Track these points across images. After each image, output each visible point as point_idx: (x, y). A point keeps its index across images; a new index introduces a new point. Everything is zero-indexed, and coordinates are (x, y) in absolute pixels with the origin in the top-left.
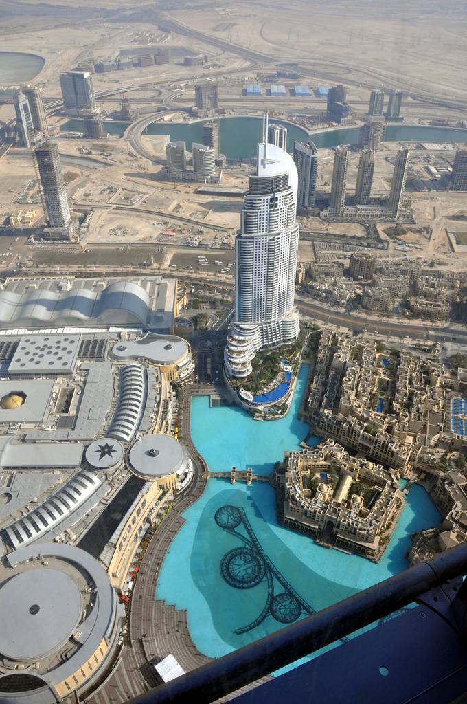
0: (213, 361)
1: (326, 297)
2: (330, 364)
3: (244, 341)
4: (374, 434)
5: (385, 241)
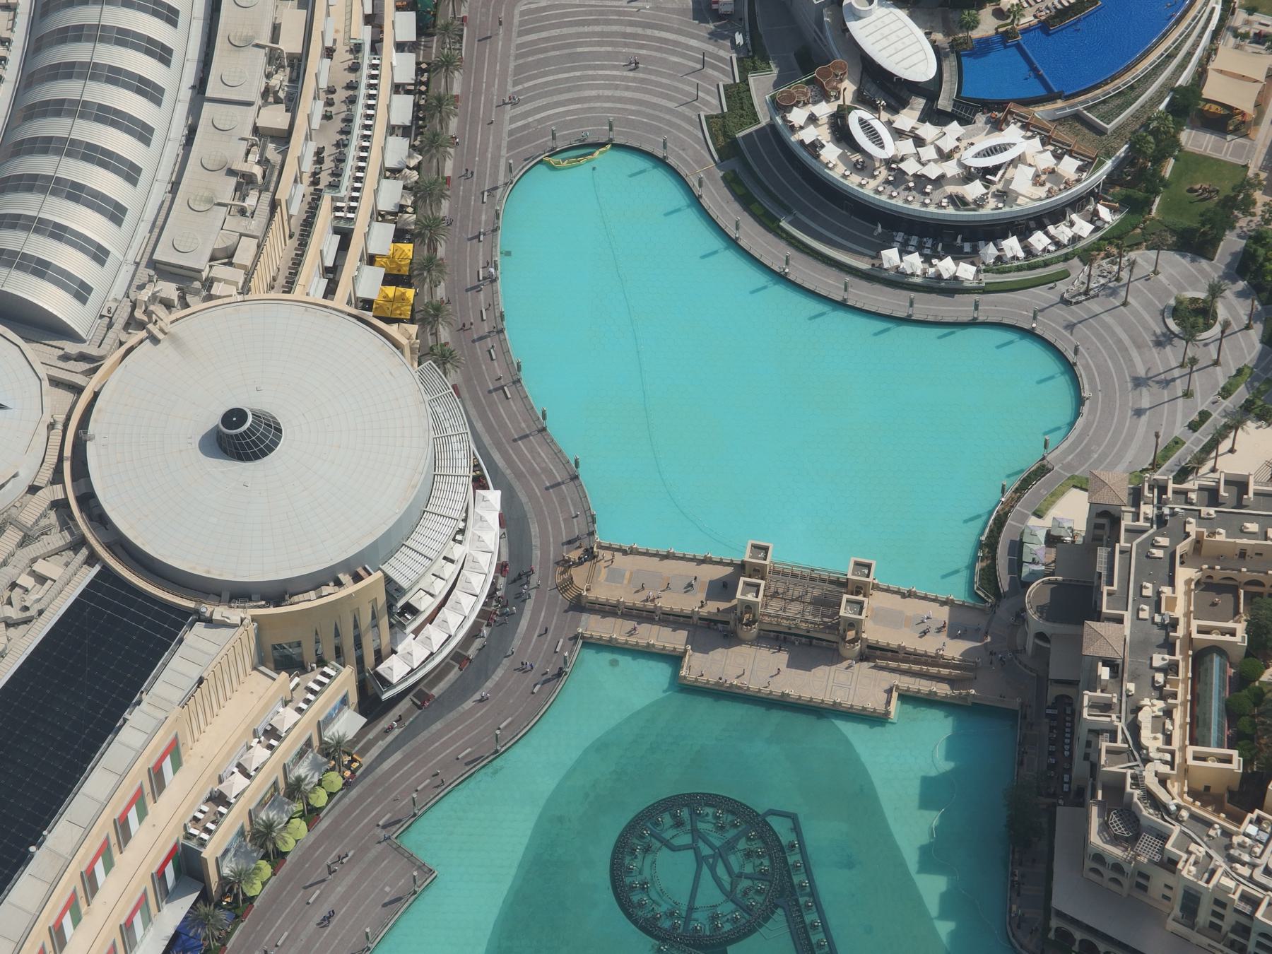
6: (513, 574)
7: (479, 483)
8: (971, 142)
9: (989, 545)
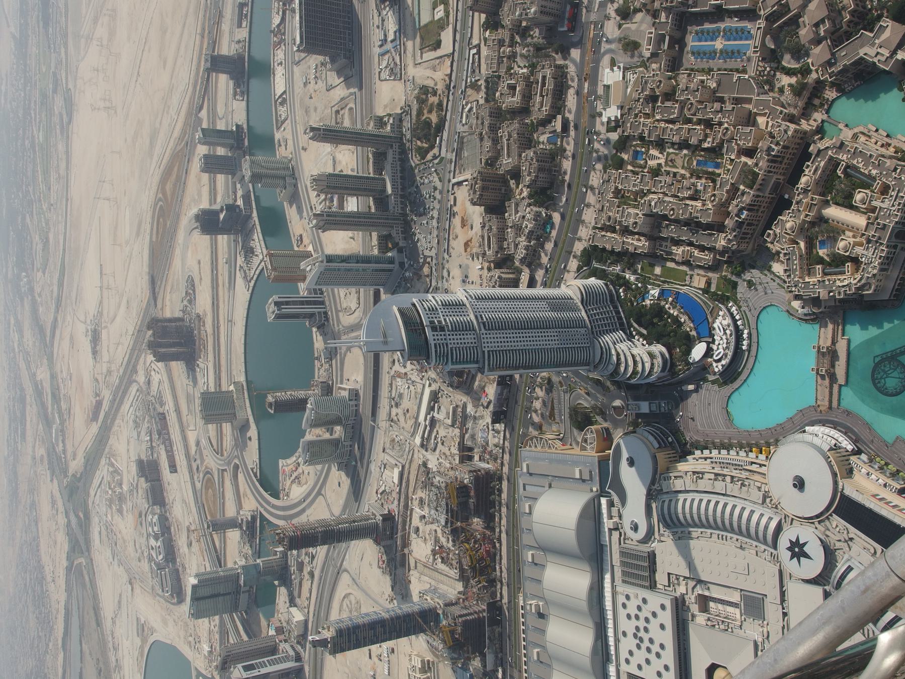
1: (538, 239)
3: (618, 355)
4: (756, 175)
6: (823, 423)
7: (804, 432)
8: (718, 334)
9: (805, 320)
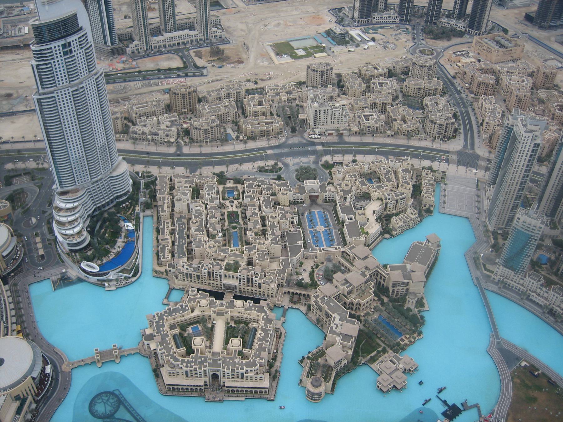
0: (43, 241)
2: (173, 210)
4: (236, 270)
5: (204, 68)
